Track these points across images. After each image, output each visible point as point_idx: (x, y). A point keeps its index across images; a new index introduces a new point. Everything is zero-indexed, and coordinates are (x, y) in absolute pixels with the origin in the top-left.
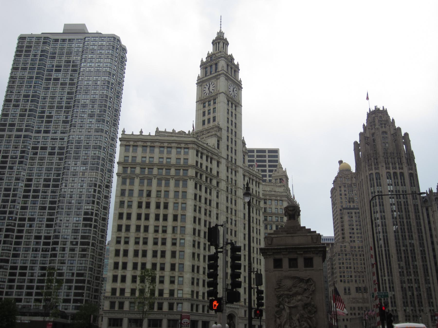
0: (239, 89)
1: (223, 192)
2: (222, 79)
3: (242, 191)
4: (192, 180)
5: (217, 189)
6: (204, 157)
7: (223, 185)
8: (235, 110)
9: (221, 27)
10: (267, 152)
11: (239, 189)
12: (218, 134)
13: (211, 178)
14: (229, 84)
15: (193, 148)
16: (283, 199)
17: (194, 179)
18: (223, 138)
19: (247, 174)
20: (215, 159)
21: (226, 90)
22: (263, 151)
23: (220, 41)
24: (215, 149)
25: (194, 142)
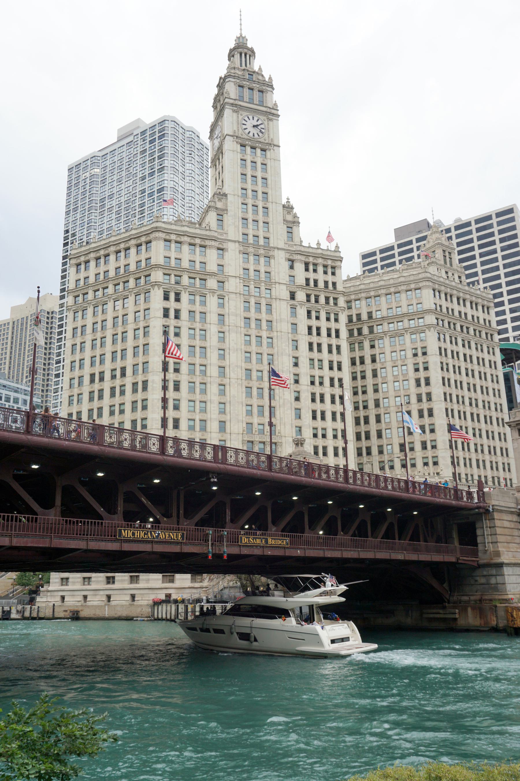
0: (271, 120)
1: (232, 296)
2: (228, 112)
3: (284, 287)
4: (156, 287)
9: (241, 29)
10: (494, 216)
11: (277, 285)
12: (219, 205)
13: (203, 277)
14: (240, 117)
15: (156, 238)
16: (421, 285)
17: (159, 286)
18: (229, 208)
19: (295, 257)
20: (211, 247)
21: (235, 128)
22: (489, 218)
23: (241, 51)
24: (210, 230)
25: (156, 227)
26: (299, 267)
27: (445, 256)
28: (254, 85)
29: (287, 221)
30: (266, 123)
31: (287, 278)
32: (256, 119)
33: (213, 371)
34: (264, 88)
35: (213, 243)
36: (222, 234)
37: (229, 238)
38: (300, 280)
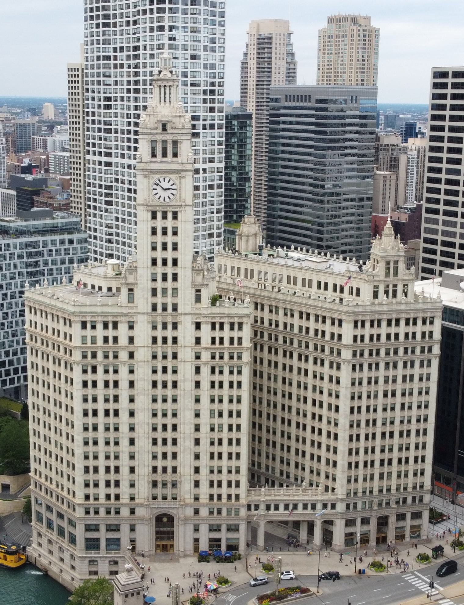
0: (183, 177)
3: (189, 350)
5: (131, 361)
6: (100, 326)
7: (143, 354)
8: (175, 217)
14: (152, 182)
18: (139, 282)
20: (121, 322)
26: (206, 329)
27: (388, 269)
28: (168, 137)
29: (195, 285)
30: (177, 182)
31: (194, 341)
32: (167, 180)
33: (124, 429)
34: (179, 137)
35: (123, 319)
36: (132, 308)
37: (139, 311)
38: (206, 341)
